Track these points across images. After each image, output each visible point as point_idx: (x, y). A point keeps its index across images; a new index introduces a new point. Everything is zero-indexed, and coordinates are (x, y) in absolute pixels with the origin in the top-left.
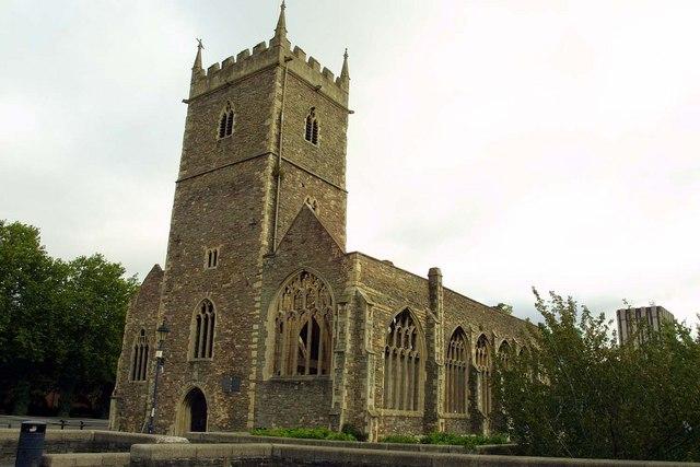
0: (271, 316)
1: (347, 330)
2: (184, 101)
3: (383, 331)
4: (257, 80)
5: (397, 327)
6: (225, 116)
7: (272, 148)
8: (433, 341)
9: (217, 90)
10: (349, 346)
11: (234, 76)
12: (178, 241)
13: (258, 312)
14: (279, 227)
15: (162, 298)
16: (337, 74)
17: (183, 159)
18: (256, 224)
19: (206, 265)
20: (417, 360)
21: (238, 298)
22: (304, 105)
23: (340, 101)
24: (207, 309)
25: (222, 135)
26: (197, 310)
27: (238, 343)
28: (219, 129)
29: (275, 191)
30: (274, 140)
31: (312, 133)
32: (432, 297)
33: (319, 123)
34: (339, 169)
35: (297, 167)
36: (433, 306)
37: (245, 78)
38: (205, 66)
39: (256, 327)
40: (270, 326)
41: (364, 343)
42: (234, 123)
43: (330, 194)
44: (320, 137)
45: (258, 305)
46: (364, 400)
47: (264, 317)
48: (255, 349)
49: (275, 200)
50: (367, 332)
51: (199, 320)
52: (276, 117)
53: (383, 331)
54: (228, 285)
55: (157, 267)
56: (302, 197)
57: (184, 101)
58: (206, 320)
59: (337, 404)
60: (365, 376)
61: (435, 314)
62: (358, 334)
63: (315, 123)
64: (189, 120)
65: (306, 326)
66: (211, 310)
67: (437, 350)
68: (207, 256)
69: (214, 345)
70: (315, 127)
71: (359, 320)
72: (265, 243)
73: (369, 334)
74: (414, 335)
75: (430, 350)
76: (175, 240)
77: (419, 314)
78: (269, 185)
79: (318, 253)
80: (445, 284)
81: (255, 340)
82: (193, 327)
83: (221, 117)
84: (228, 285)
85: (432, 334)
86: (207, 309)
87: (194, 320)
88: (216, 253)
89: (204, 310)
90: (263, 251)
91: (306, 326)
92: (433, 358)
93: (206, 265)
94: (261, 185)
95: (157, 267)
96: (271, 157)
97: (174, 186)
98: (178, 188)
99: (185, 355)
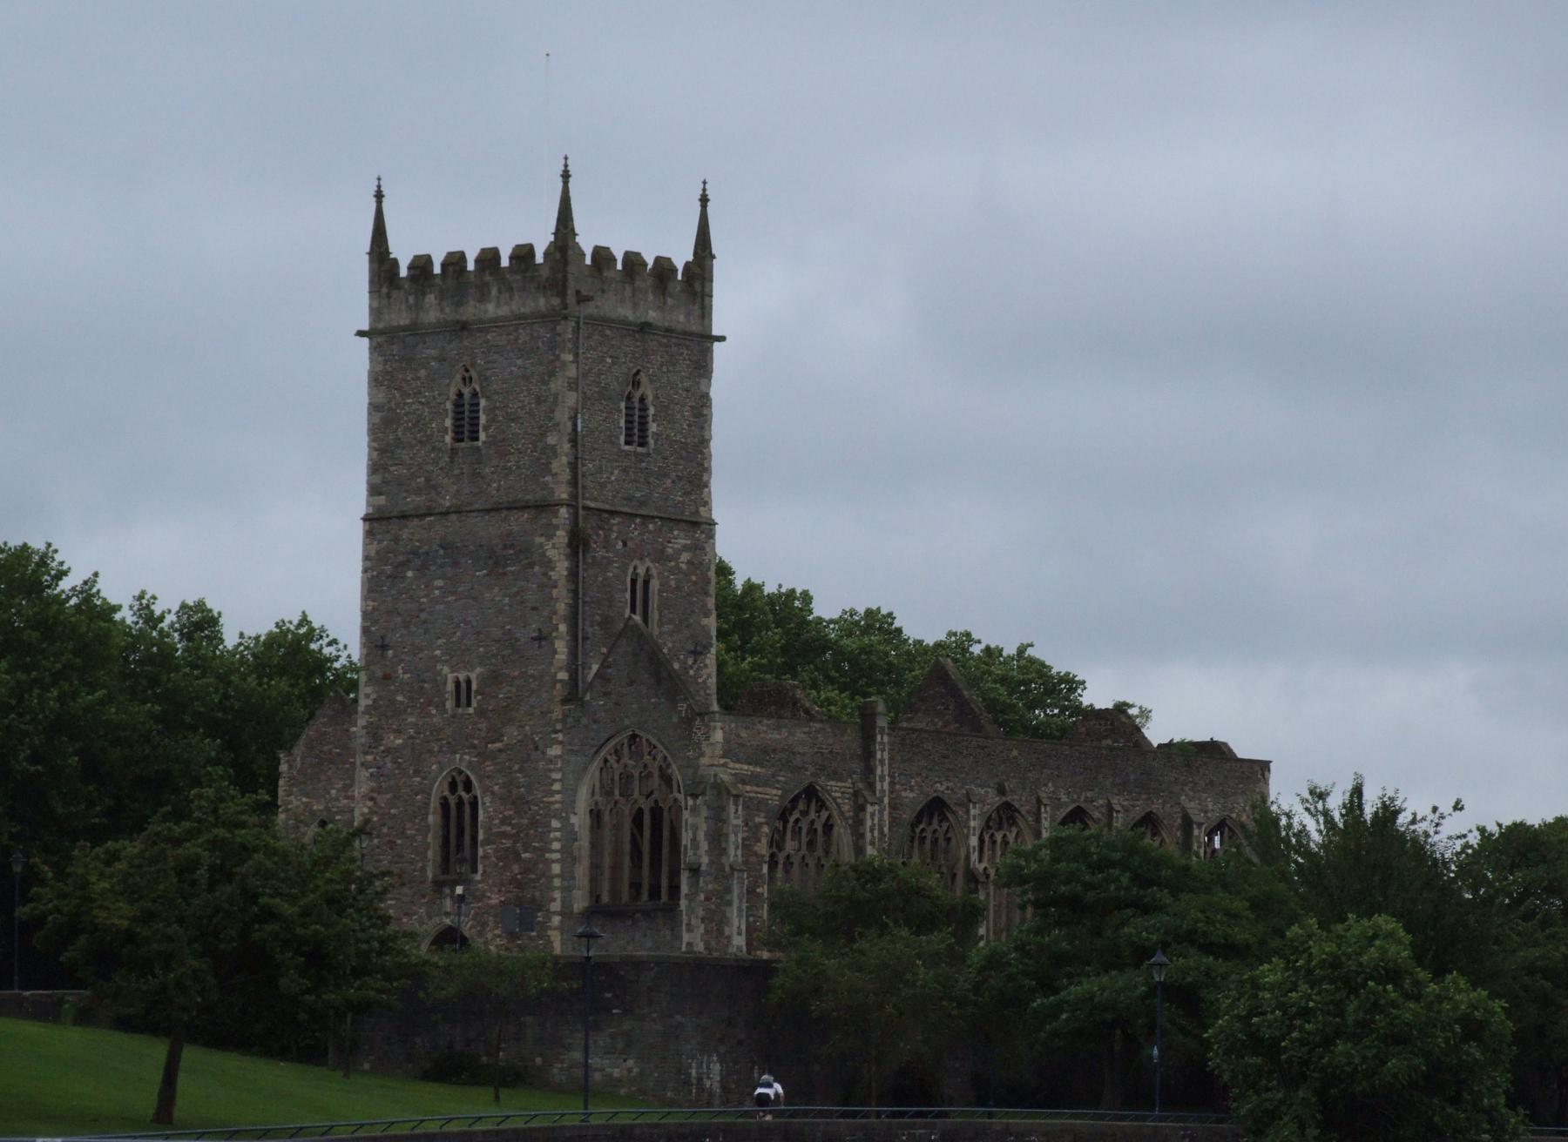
6: (460, 395)
19: (449, 705)
26: (439, 788)
28: (448, 423)
31: (637, 432)
35: (613, 513)
36: (869, 770)
42: (483, 419)
51: (445, 804)
58: (460, 803)
66: (468, 786)
68: (450, 686)
81: (556, 845)
88: (469, 682)
89: (453, 786)
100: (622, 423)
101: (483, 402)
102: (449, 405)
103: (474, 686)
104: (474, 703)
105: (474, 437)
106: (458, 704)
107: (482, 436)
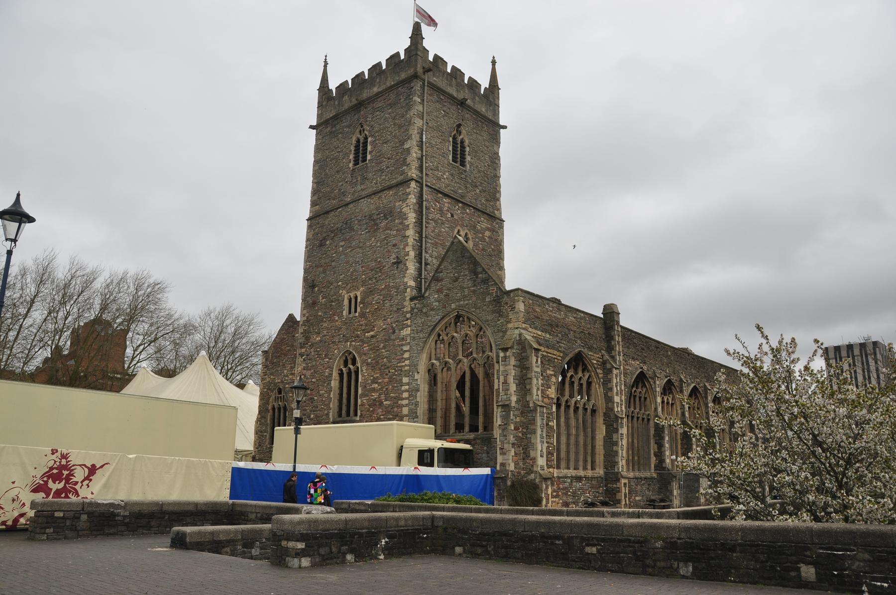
0: (422, 367)
1: (511, 380)
2: (311, 127)
3: (554, 379)
4: (392, 96)
5: (569, 375)
6: (358, 141)
7: (413, 173)
8: (611, 389)
9: (347, 112)
10: (514, 399)
11: (365, 95)
12: (313, 286)
13: (407, 362)
14: (426, 264)
15: (299, 351)
16: (485, 83)
17: (314, 193)
18: (399, 262)
20: (594, 411)
21: (384, 347)
22: (447, 124)
23: (490, 115)
24: (350, 362)
25: (356, 163)
26: (337, 364)
27: (386, 400)
28: (352, 157)
29: (419, 223)
30: (415, 165)
31: (459, 155)
32: (609, 338)
33: (467, 143)
34: (494, 194)
36: (610, 349)
37: (378, 95)
38: (333, 85)
39: (405, 380)
40: (421, 378)
41: (531, 394)
42: (369, 148)
43: (484, 223)
44: (468, 158)
45: (406, 355)
46: (534, 459)
47: (414, 367)
48: (407, 405)
49: (420, 233)
50: (534, 381)
51: (341, 374)
52: (415, 137)
53: (554, 379)
54: (372, 333)
55: (291, 318)
56: (452, 228)
57: (311, 127)
58: (349, 374)
59: (503, 465)
60: (534, 432)
61: (613, 358)
62: (523, 383)
63: (462, 142)
64: (318, 149)
65: (463, 376)
67: (617, 399)
68: (346, 302)
69: (359, 401)
70: (463, 147)
71: (523, 367)
72: (412, 283)
73: (536, 383)
74: (589, 384)
75: (609, 400)
76: (310, 285)
77: (594, 358)
78: (412, 217)
79: (474, 292)
80: (623, 322)
82: (335, 384)
83: (354, 142)
84: (372, 333)
85: (610, 381)
86: (350, 362)
87: (335, 374)
88: (356, 298)
90: (409, 293)
91: (463, 376)
92: (612, 409)
93: (345, 313)
94: (403, 216)
95: (291, 318)
96: (413, 184)
97: (305, 224)
98: (310, 227)
99: (328, 414)
100: (451, 148)
101: (369, 139)
102: (353, 148)
103: (359, 300)
104: (358, 310)
105: (364, 160)
106: (350, 313)
107: (369, 157)
